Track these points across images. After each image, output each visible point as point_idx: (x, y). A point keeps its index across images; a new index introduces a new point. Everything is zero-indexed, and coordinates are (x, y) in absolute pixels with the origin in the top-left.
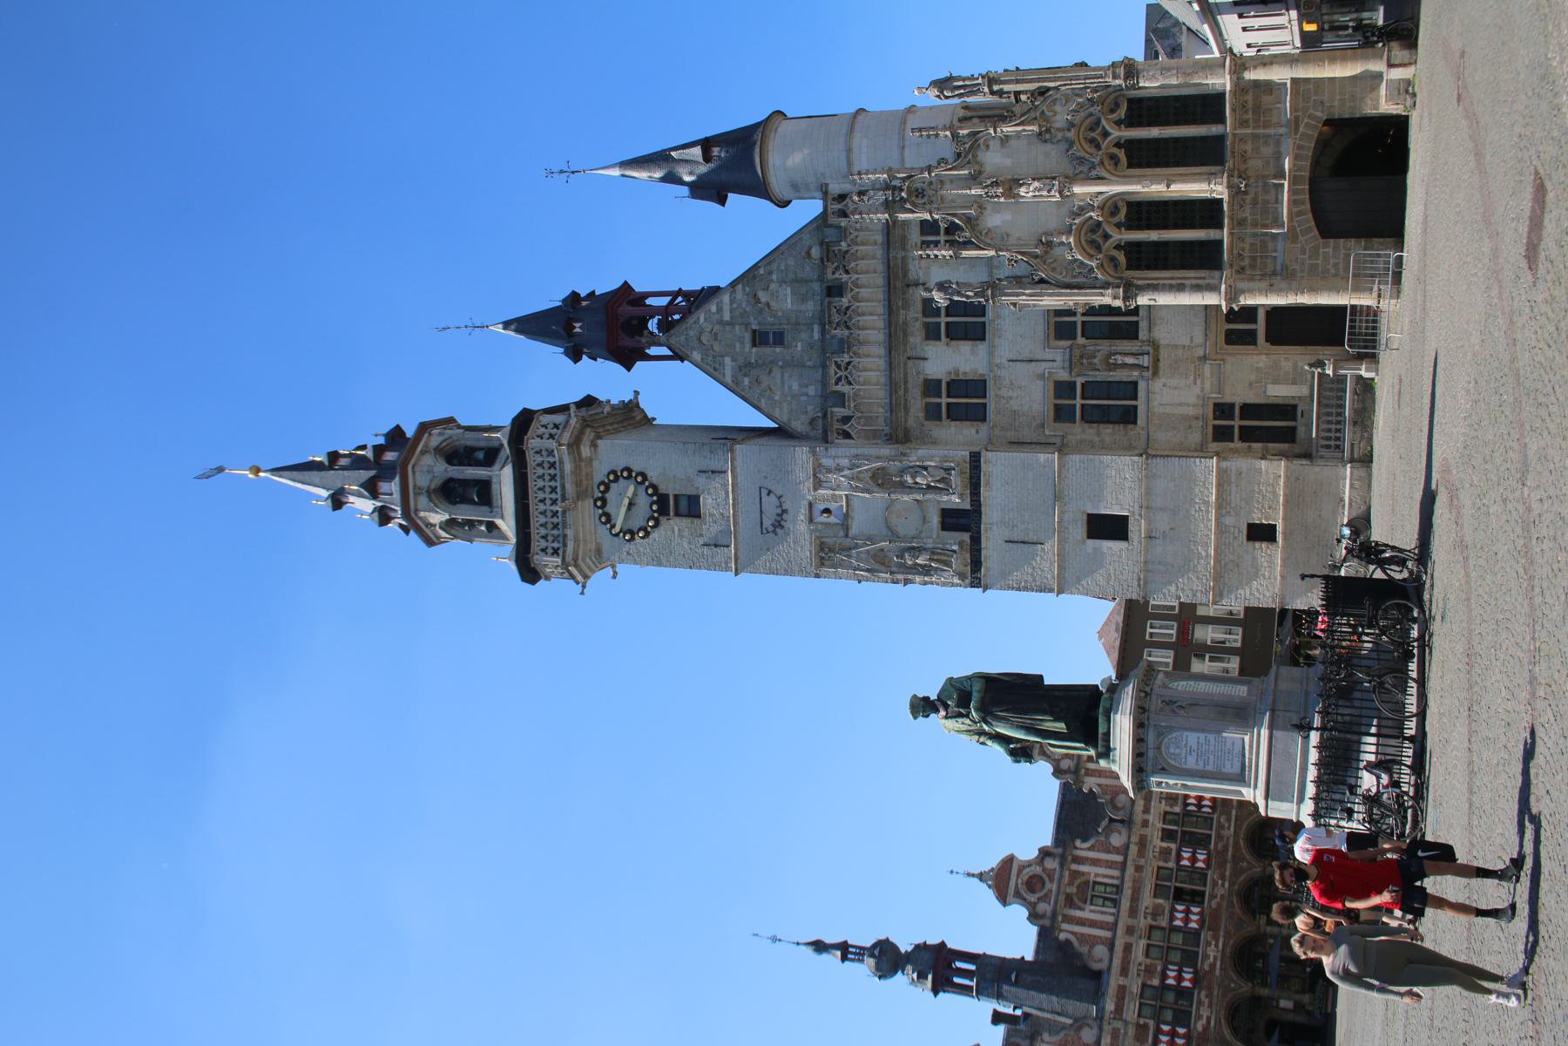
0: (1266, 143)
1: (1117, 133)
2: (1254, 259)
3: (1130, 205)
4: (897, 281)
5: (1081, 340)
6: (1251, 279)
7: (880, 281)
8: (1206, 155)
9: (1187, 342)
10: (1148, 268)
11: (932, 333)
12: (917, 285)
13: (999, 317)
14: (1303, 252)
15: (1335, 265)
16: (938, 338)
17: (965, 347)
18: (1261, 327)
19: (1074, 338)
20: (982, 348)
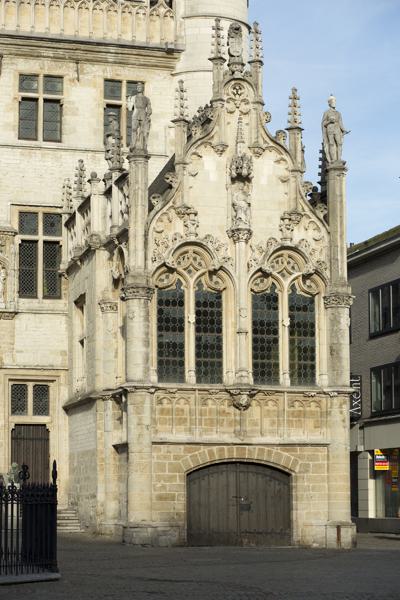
0: (273, 423)
1: (286, 283)
2: (169, 412)
3: (219, 295)
4: (84, 50)
5: (18, 239)
6: (153, 411)
7: (84, 35)
8: (264, 368)
9: (17, 346)
10: (160, 312)
11: (26, 80)
12: (77, 71)
13: (43, 155)
14: (176, 458)
15: (164, 487)
16: (21, 89)
17: (13, 117)
18: (30, 418)
19: (22, 230)
20: (12, 137)
